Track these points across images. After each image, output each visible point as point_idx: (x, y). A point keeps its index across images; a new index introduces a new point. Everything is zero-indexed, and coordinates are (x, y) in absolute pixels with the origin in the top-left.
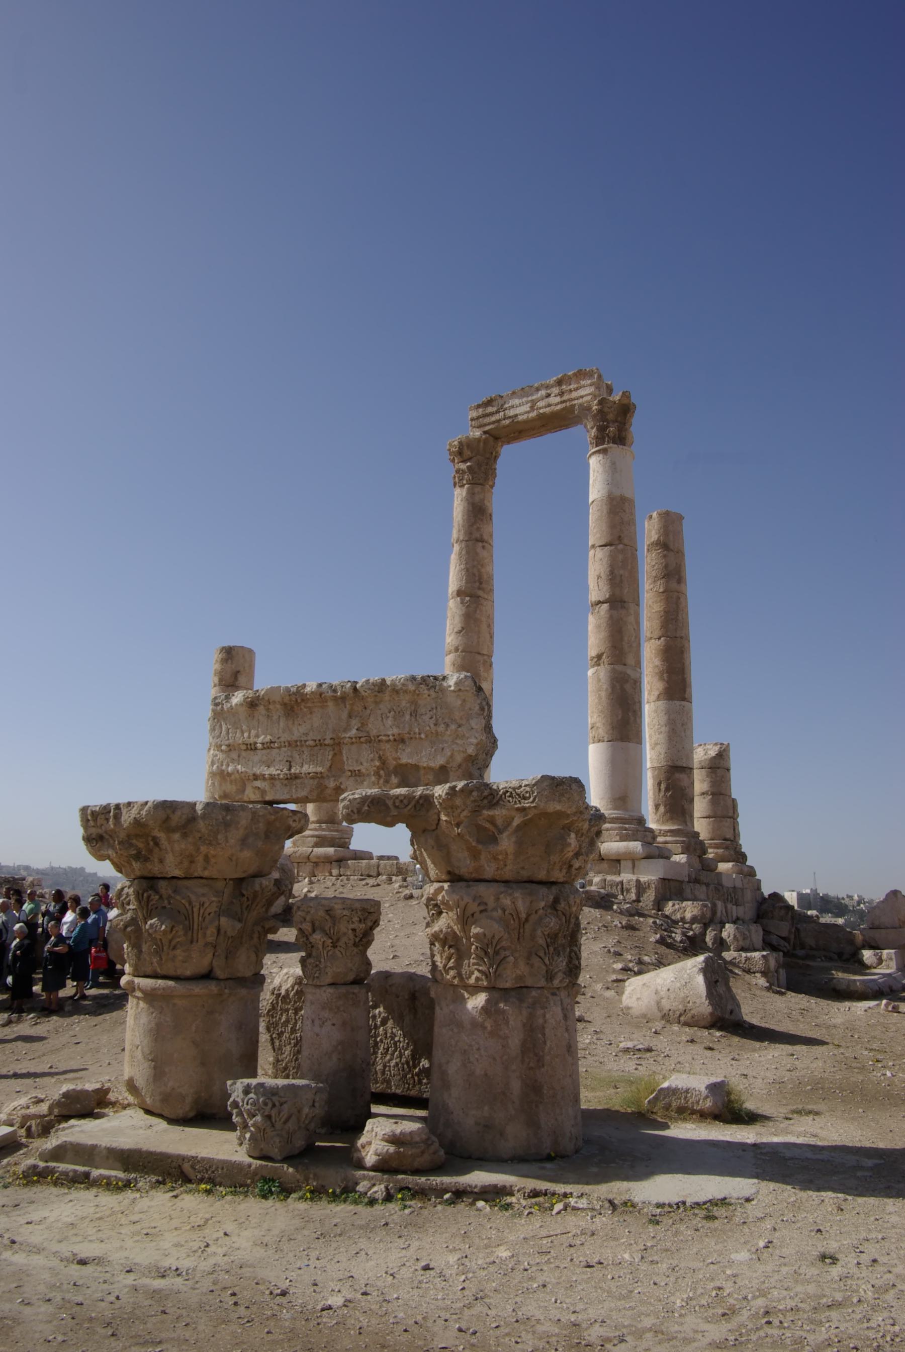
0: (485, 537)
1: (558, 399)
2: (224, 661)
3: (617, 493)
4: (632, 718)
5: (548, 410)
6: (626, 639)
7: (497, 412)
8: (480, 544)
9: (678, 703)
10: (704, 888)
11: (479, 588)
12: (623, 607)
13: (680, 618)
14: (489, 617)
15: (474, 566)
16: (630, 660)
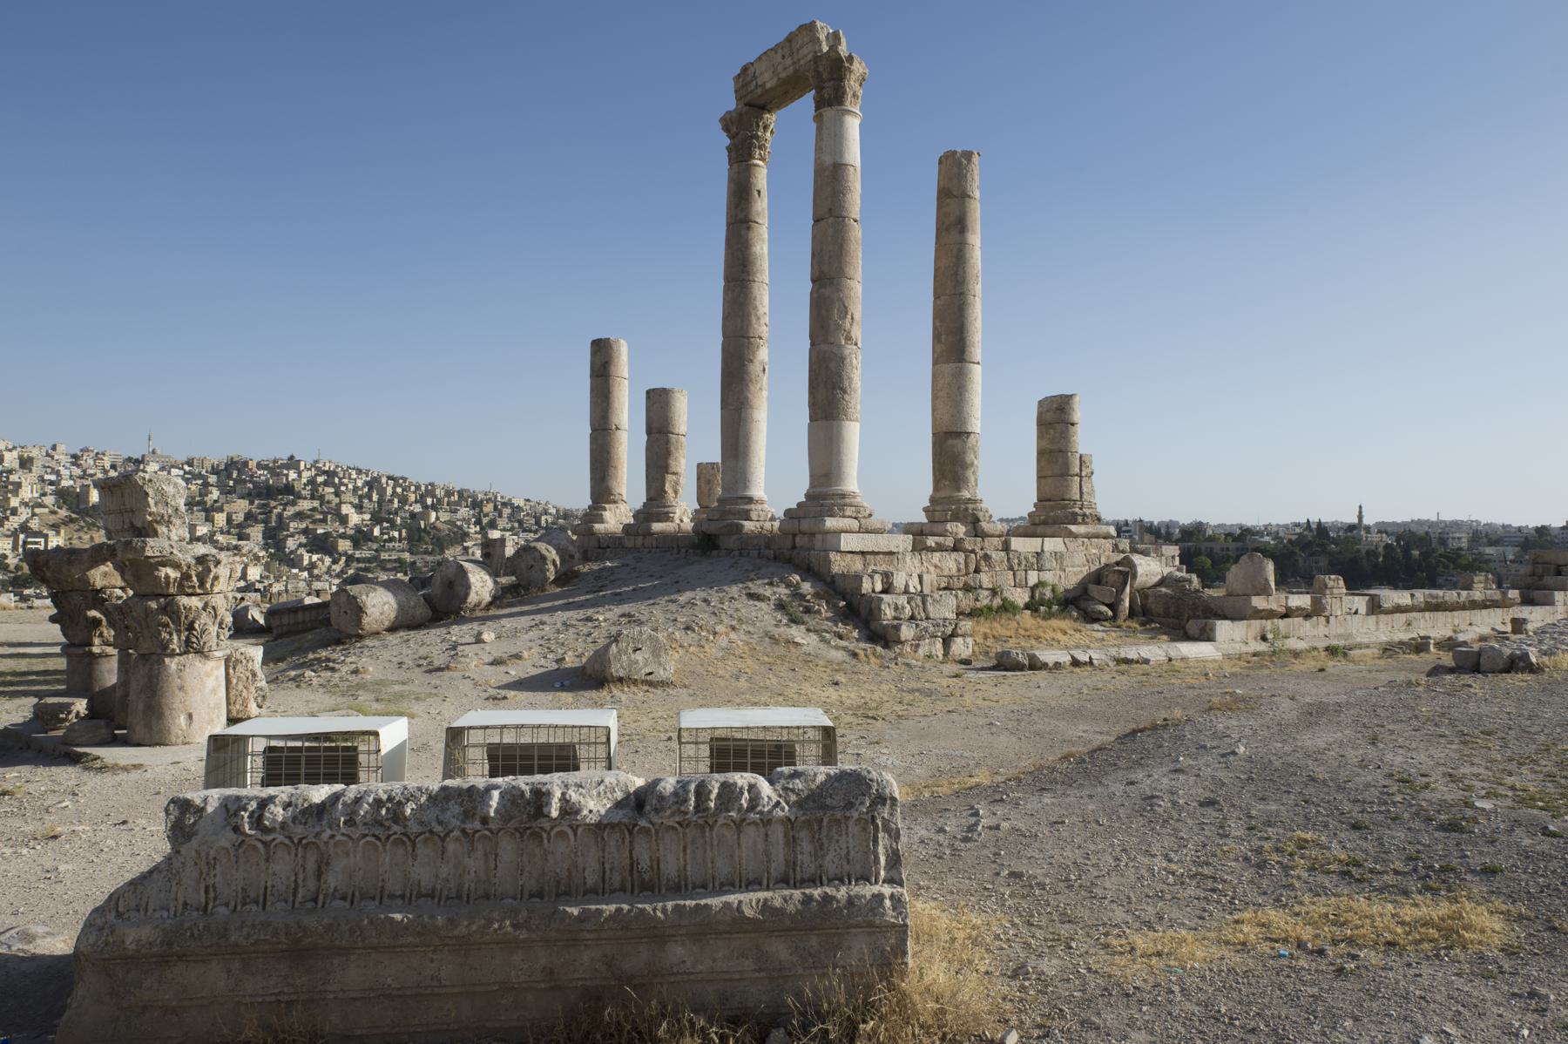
1: (788, 61)
3: (828, 161)
5: (783, 75)
10: (961, 557)
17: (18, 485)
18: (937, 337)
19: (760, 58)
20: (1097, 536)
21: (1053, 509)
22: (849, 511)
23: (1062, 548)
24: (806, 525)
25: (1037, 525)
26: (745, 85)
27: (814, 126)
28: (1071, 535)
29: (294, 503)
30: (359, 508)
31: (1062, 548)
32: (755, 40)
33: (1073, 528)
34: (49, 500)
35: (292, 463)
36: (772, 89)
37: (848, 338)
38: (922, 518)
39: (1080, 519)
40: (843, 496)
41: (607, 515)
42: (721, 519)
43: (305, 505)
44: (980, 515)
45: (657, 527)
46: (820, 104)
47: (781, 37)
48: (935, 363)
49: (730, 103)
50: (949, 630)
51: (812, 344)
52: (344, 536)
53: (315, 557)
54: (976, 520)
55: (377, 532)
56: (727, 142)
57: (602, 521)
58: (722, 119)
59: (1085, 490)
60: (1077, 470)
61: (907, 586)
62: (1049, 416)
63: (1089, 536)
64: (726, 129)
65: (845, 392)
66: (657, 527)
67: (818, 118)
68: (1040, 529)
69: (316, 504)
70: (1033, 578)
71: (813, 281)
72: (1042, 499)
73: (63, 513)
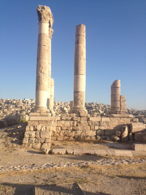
17: (56, 108)
20: (124, 117)
22: (38, 111)
28: (113, 117)
30: (102, 110)
33: (114, 115)
34: (59, 110)
35: (93, 103)
37: (41, 72)
39: (118, 113)
43: (94, 110)
44: (80, 112)
50: (43, 141)
54: (79, 113)
55: (105, 114)
59: (122, 105)
61: (41, 129)
65: (40, 84)
69: (95, 110)
70: (97, 128)
73: (61, 111)
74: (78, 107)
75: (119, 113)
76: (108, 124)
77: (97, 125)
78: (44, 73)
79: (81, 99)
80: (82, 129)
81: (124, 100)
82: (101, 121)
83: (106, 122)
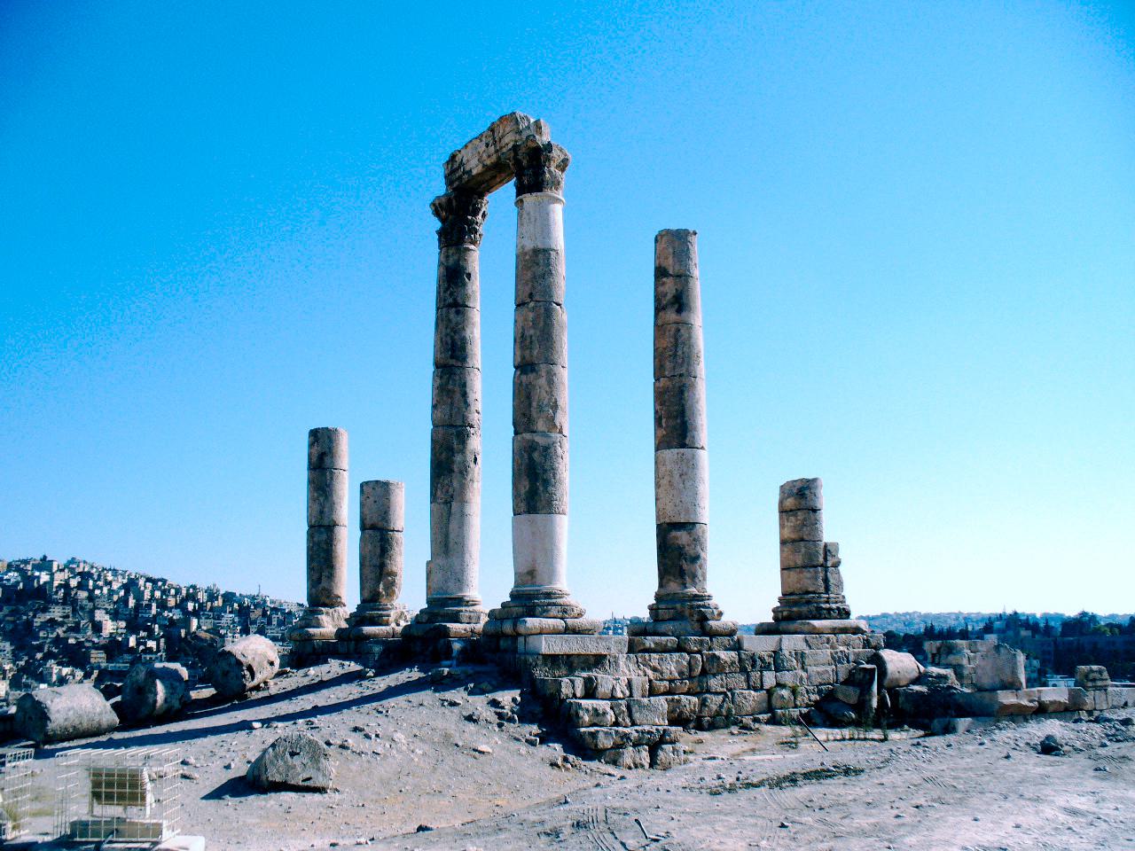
0: (460, 301)
1: (492, 149)
2: (311, 445)
3: (529, 245)
4: (541, 488)
5: (488, 162)
6: (534, 404)
7: (459, 167)
8: (454, 309)
9: (675, 451)
11: (452, 357)
12: (533, 370)
13: (680, 353)
14: (464, 385)
15: (447, 335)
16: (541, 425)
18: (658, 421)
19: (466, 146)
21: (796, 603)
22: (554, 611)
23: (802, 646)
24: (508, 628)
25: (783, 622)
26: (453, 171)
27: (516, 210)
29: (45, 610)
30: (115, 616)
31: (802, 646)
32: (460, 131)
33: (816, 623)
35: (45, 564)
36: (478, 175)
38: (644, 615)
40: (549, 595)
41: (324, 618)
42: (430, 621)
45: (368, 629)
46: (521, 190)
47: (484, 127)
48: (657, 449)
49: (440, 188)
51: (516, 433)
52: (97, 647)
53: (66, 671)
54: (703, 619)
55: (132, 642)
56: (438, 225)
57: (318, 625)
58: (433, 204)
60: (821, 560)
62: (790, 502)
63: (835, 631)
64: (437, 213)
66: (368, 629)
67: (519, 203)
68: (783, 625)
70: (770, 679)
71: (516, 367)
72: (788, 598)
74: (693, 590)
75: (829, 613)
76: (803, 663)
77: (767, 668)
78: (561, 432)
79: (702, 555)
80: (722, 690)
81: (835, 560)
82: (781, 649)
83: (796, 654)
